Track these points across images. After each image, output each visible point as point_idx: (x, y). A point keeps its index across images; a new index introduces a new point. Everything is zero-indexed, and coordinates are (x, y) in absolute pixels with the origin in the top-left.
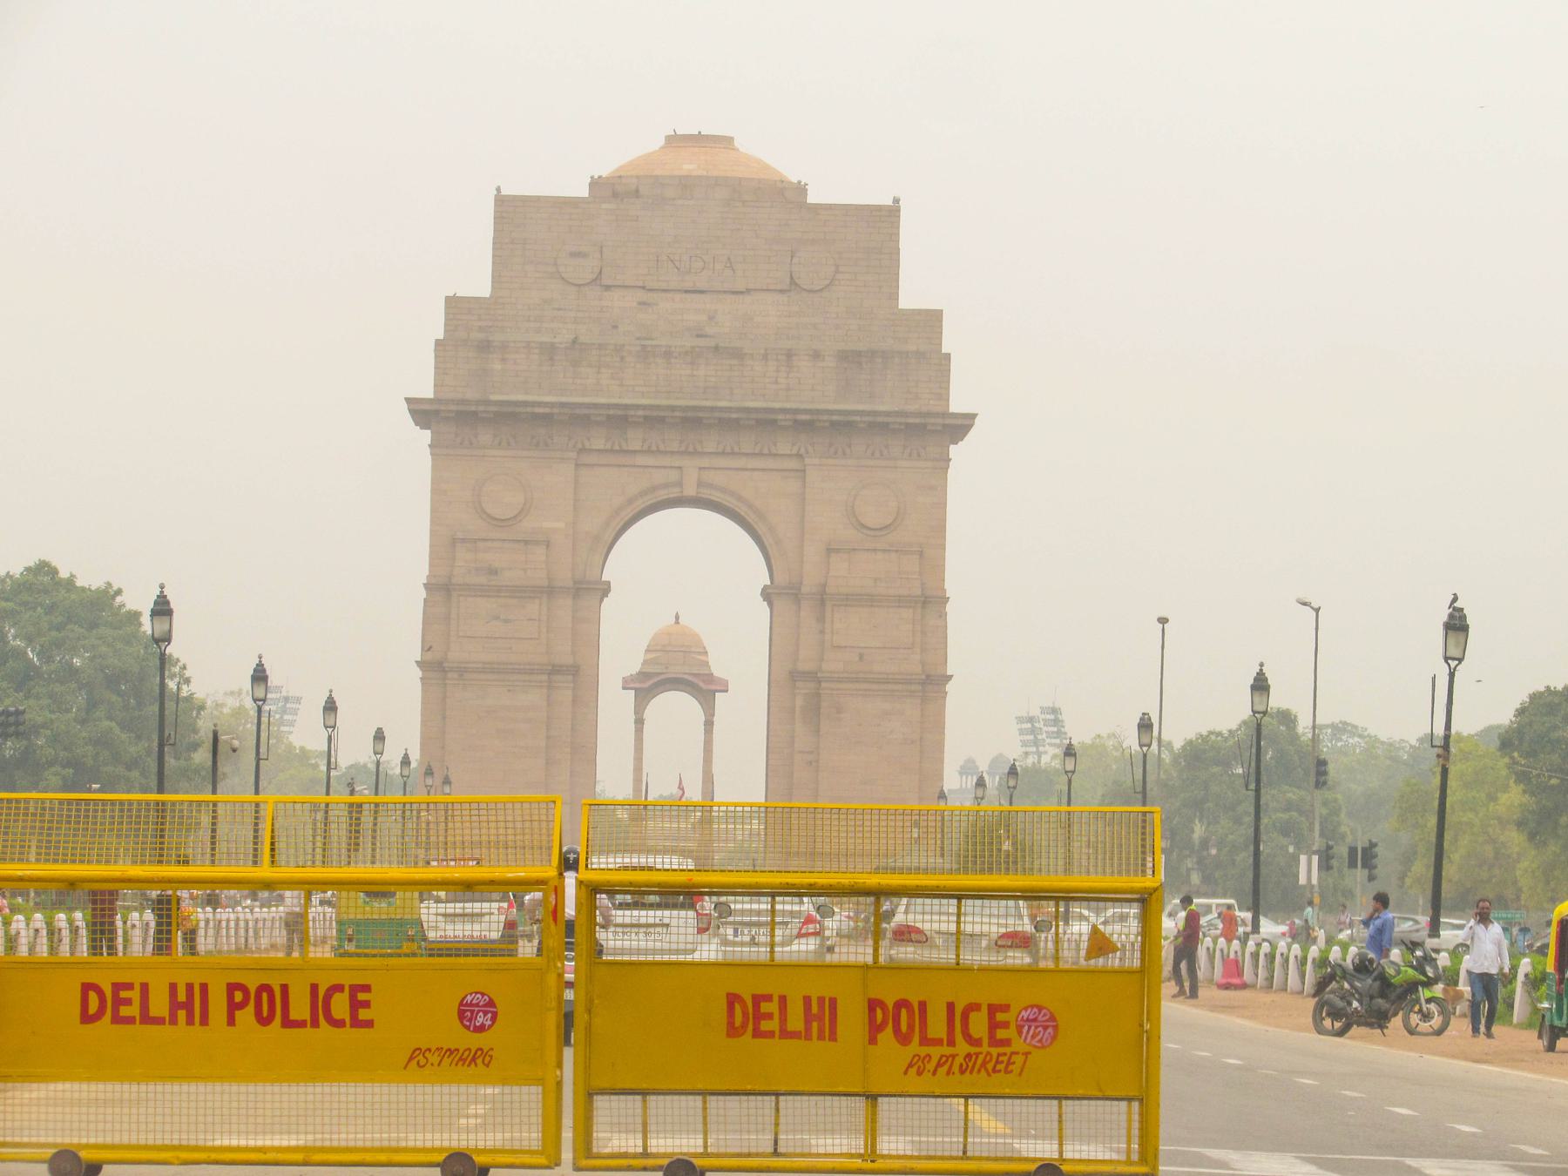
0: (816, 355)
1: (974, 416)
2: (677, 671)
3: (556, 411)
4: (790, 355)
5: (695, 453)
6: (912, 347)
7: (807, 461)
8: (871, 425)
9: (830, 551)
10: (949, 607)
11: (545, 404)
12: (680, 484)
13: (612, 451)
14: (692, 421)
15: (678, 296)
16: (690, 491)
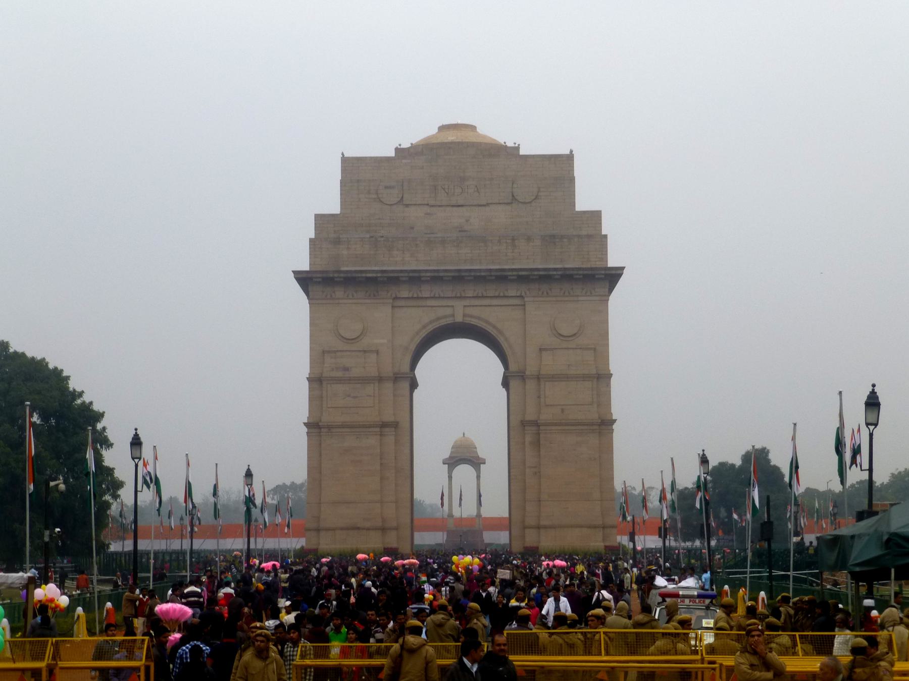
0: (529, 239)
1: (623, 268)
2: (464, 456)
3: (379, 275)
4: (513, 240)
5: (461, 298)
6: (584, 233)
7: (526, 299)
8: (562, 276)
9: (541, 350)
10: (613, 381)
11: (373, 271)
12: (453, 316)
13: (412, 298)
14: (459, 278)
15: (448, 209)
16: (459, 319)
